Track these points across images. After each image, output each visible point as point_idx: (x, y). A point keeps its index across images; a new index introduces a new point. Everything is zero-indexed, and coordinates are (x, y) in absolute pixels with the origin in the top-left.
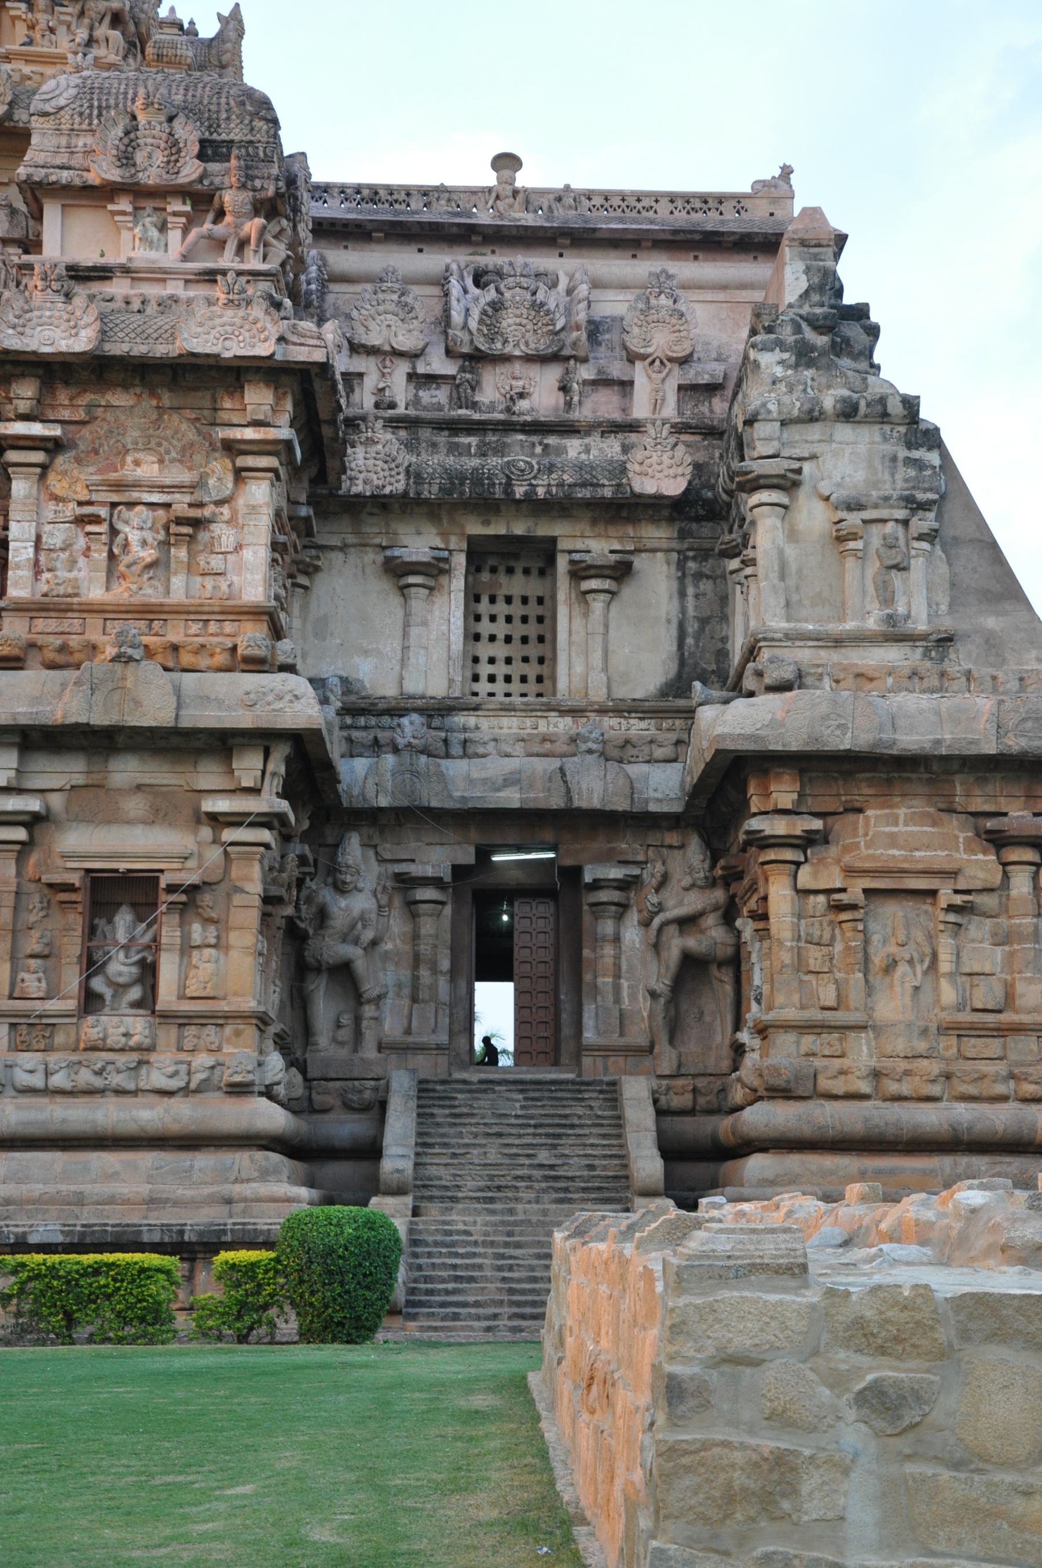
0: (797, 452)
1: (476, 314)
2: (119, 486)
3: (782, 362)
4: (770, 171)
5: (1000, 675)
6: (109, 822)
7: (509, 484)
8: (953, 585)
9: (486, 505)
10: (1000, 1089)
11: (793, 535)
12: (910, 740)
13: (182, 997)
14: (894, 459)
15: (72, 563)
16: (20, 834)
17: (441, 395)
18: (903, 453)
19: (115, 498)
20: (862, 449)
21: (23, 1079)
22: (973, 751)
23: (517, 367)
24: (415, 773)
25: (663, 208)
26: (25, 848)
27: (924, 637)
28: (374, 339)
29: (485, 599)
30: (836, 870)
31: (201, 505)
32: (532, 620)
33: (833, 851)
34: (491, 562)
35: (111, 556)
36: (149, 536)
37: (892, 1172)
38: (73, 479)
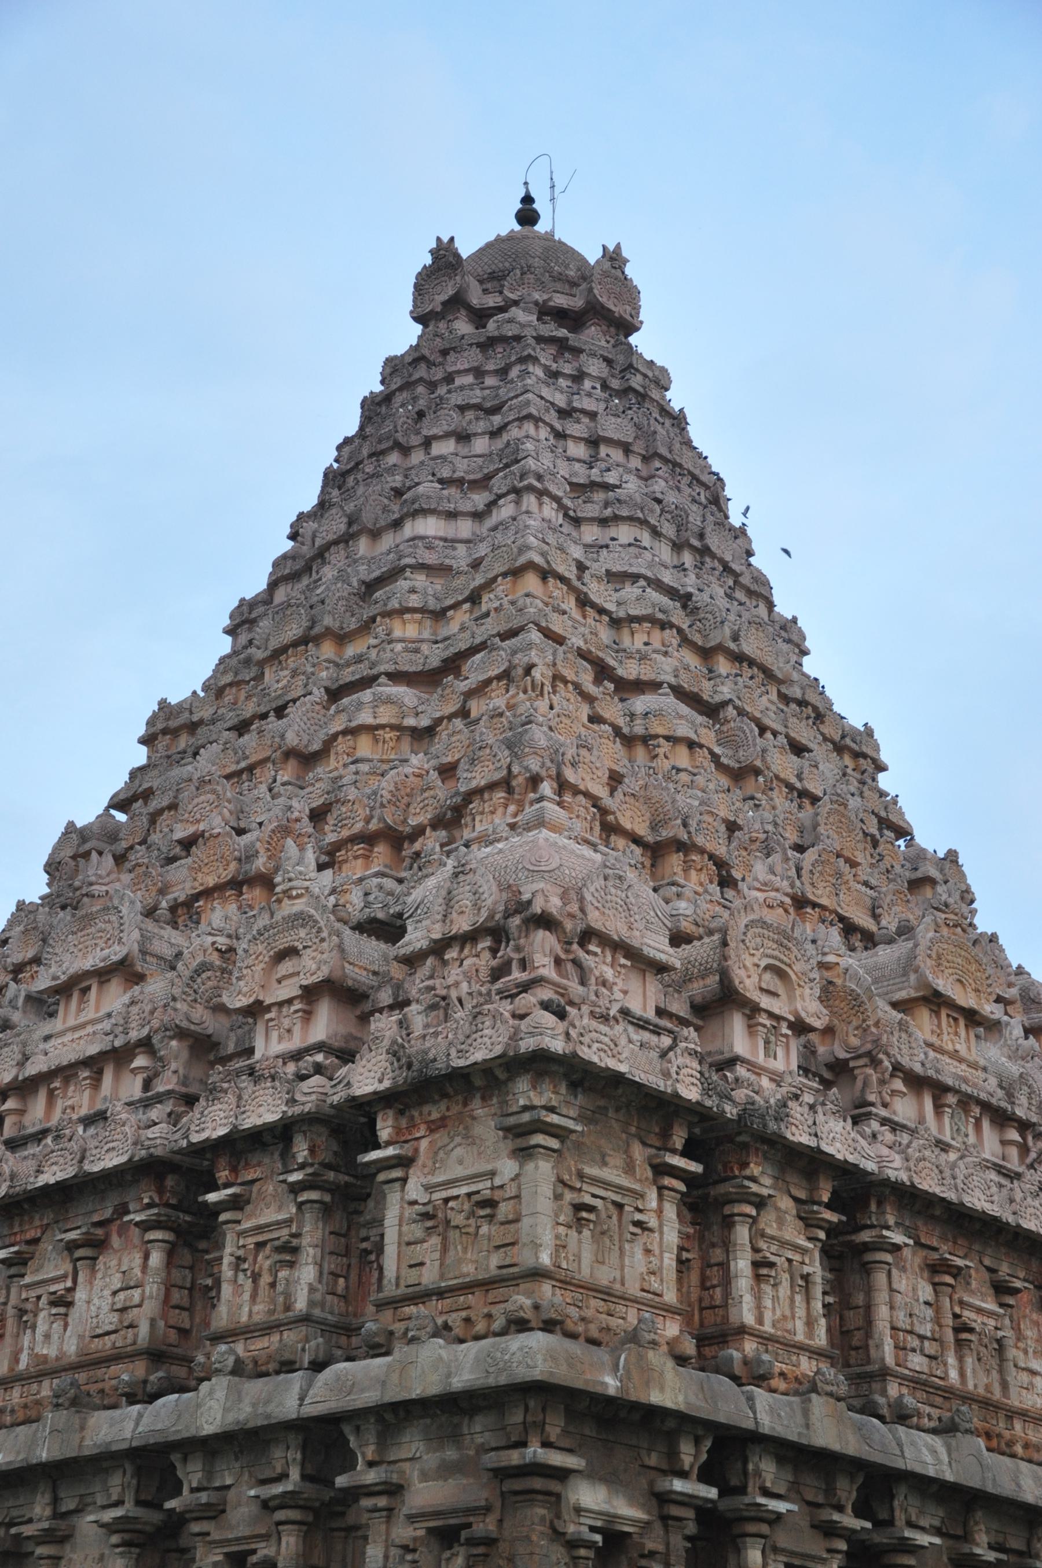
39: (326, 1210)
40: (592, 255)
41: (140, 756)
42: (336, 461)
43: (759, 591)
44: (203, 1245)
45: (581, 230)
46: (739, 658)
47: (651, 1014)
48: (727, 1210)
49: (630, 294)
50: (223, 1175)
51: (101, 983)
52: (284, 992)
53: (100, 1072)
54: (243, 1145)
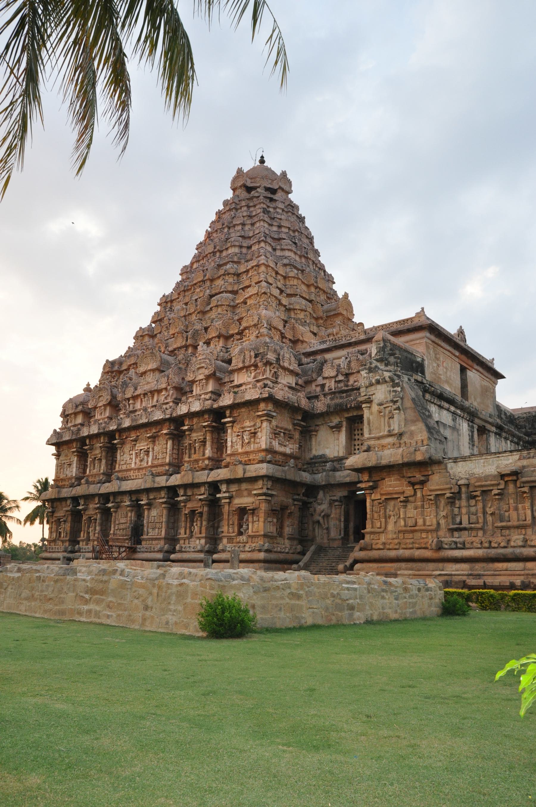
0: (370, 393)
1: (346, 364)
2: (243, 428)
3: (366, 373)
4: (419, 310)
5: (412, 442)
6: (241, 497)
7: (346, 405)
8: (405, 420)
9: (347, 410)
10: (411, 546)
11: (371, 413)
12: (384, 462)
13: (252, 532)
14: (390, 391)
15: (237, 444)
16: (228, 501)
17: (342, 384)
18: (392, 389)
19: (243, 430)
20: (383, 390)
21: (228, 549)
22: (397, 463)
23: (355, 375)
24: (329, 476)
25: (395, 326)
26: (229, 503)
27: (396, 434)
28: (326, 375)
29: (356, 430)
30: (379, 494)
31: (256, 429)
32: (360, 435)
33: (379, 489)
34: (357, 421)
35: (243, 442)
36: (248, 437)
37: (384, 567)
38: (237, 427)
39: (212, 432)
40: (278, 173)
41: (158, 308)
42: (210, 227)
43: (322, 268)
44: (180, 439)
45: (275, 165)
46: (317, 287)
47: (294, 385)
48: (311, 433)
49: (289, 183)
50: (187, 423)
51: (153, 373)
52: (201, 377)
53: (154, 394)
54: (191, 415)
